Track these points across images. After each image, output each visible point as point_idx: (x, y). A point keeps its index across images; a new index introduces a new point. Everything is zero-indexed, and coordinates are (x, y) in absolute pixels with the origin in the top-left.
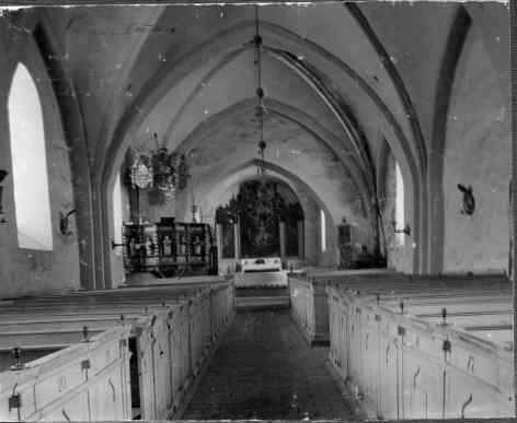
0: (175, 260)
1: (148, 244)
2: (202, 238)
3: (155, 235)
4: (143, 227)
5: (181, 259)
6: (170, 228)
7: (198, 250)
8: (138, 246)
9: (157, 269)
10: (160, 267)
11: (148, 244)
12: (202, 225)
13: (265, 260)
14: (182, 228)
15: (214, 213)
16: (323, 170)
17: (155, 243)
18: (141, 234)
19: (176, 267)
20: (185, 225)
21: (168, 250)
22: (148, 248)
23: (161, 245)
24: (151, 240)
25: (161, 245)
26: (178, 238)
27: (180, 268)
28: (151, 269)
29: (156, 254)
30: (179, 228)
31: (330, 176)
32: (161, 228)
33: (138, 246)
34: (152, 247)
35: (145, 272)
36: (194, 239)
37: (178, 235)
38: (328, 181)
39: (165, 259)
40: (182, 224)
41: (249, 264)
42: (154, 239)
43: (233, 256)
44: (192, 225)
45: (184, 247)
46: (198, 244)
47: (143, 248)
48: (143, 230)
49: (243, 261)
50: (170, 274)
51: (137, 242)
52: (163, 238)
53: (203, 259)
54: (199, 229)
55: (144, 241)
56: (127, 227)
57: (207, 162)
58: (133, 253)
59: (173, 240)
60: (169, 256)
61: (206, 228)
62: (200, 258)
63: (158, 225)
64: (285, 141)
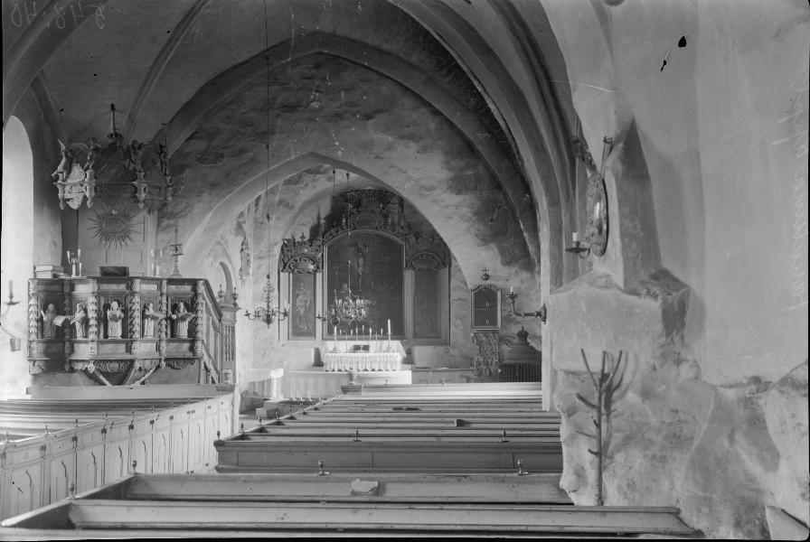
0: (129, 350)
1: (79, 315)
2: (192, 306)
3: (92, 299)
4: (72, 285)
5: (143, 349)
6: (122, 287)
7: (183, 329)
8: (59, 321)
9: (92, 368)
10: (96, 362)
11: (79, 315)
12: (194, 283)
13: (373, 344)
14: (154, 287)
15: (277, 250)
16: (445, 174)
17: (91, 315)
18: (71, 296)
19: (132, 361)
20: (159, 281)
21: (116, 330)
22: (78, 326)
23: (103, 321)
24: (86, 311)
25: (103, 321)
26: (137, 307)
27: (137, 365)
28: (79, 366)
29: (92, 337)
30: (138, 286)
31: (458, 185)
32: (105, 287)
33: (59, 321)
34: (85, 321)
35: (72, 370)
36: (175, 308)
37: (137, 299)
38: (454, 199)
39: (108, 348)
40: (145, 279)
41: (340, 352)
42: (91, 308)
43: (312, 334)
44: (170, 281)
45: (150, 326)
46: (183, 319)
47: (69, 327)
48: (72, 288)
49: (330, 345)
50: (120, 378)
51: (59, 312)
52: (107, 307)
53: (192, 349)
54: (188, 288)
55: (71, 313)
56: (41, 282)
58: (49, 333)
60: (115, 342)
61: (201, 289)
62: (186, 346)
63: (99, 281)
64: (368, 117)
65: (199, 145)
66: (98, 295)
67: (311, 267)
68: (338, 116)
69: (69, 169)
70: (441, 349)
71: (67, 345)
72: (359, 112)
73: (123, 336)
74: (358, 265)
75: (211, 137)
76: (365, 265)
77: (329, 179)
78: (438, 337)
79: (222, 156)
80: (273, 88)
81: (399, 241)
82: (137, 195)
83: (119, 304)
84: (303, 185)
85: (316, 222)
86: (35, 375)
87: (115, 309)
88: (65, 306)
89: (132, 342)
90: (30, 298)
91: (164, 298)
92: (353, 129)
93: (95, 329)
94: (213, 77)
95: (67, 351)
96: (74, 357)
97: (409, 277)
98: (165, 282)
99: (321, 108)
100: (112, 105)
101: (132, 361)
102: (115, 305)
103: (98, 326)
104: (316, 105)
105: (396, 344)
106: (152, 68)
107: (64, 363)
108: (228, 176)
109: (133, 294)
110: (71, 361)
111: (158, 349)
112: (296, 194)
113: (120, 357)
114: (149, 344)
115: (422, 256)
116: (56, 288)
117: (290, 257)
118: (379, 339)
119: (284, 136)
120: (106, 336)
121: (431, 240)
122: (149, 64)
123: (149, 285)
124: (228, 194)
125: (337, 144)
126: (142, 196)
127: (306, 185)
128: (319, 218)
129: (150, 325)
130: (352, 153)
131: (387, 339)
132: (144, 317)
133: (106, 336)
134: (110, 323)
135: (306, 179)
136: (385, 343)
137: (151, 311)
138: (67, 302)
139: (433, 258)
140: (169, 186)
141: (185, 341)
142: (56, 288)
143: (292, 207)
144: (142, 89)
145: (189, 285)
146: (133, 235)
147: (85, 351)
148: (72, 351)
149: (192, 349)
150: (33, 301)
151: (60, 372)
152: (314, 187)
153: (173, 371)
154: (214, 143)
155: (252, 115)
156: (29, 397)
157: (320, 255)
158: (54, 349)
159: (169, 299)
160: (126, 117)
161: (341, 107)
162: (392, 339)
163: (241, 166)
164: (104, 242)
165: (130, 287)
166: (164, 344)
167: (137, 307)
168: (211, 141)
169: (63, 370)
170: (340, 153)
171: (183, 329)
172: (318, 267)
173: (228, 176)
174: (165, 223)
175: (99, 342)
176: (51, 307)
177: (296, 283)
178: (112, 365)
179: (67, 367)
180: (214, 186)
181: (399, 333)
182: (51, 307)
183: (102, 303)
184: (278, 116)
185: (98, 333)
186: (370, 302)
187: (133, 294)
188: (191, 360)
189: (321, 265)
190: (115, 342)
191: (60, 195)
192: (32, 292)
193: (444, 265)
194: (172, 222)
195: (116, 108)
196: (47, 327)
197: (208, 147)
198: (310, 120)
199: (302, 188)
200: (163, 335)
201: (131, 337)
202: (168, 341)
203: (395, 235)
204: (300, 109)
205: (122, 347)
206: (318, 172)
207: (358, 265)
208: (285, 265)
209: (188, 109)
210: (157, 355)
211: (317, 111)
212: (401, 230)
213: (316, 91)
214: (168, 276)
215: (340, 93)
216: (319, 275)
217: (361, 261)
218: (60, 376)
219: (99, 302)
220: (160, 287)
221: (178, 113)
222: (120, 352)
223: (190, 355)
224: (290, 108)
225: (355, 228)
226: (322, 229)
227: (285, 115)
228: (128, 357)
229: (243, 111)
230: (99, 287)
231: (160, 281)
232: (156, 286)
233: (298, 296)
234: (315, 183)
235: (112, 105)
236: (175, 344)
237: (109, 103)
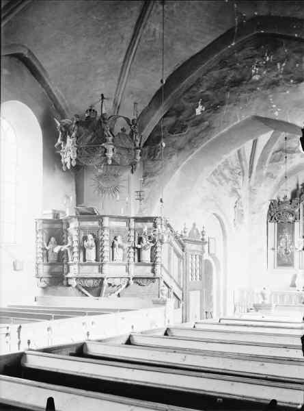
0: (101, 271)
6: (96, 224)
8: (57, 249)
14: (123, 224)
17: (76, 244)
19: (103, 279)
20: (127, 219)
21: (91, 255)
25: (83, 249)
27: (106, 282)
32: (84, 224)
36: (140, 240)
37: (106, 232)
42: (75, 239)
44: (137, 219)
52: (85, 238)
53: (153, 271)
57: (184, 128)
58: (52, 258)
59: (98, 243)
62: (150, 268)
65: (171, 121)
66: (79, 229)
67: (291, 219)
68: (274, 84)
69: (64, 140)
71: (65, 267)
72: (292, 78)
73: (96, 260)
75: (179, 113)
79: (186, 126)
80: (225, 70)
82: (106, 154)
83: (94, 236)
85: (295, 187)
86: (44, 288)
87: (91, 241)
88: (64, 238)
89: (102, 264)
90: (37, 233)
91: (132, 233)
92: (288, 92)
93: (76, 255)
94: (177, 68)
95: (65, 272)
96: (69, 275)
98: (132, 220)
99: (261, 79)
100: (102, 95)
101: (103, 279)
102: (90, 237)
103: (79, 252)
104: (256, 78)
106: (124, 62)
107: (63, 279)
108: (190, 141)
109: (103, 228)
110: (67, 278)
111: (127, 270)
112: (278, 168)
113: (94, 276)
114: (119, 267)
116: (57, 226)
117: (276, 212)
119: (231, 105)
120: (85, 260)
122: (122, 59)
123: (118, 223)
124: (190, 154)
125: (274, 106)
126: (110, 155)
128: (298, 185)
129: (119, 254)
130: (287, 112)
132: (113, 246)
133: (85, 260)
134: (87, 251)
137: (119, 242)
138: (65, 236)
140: (137, 149)
141: (148, 265)
142: (57, 226)
143: (275, 178)
144: (119, 80)
145: (151, 222)
146: (121, 189)
147: (73, 272)
148: (68, 271)
149: (153, 271)
150: (40, 235)
151: (61, 286)
152: (291, 162)
153: (140, 287)
154: (181, 117)
155: (208, 93)
156: (35, 304)
157: (297, 210)
158: (57, 269)
159: (136, 234)
160: (112, 104)
161: (277, 76)
163: (199, 133)
164: (101, 195)
165: (101, 224)
166: (132, 267)
167: (106, 238)
168: (178, 116)
169: (62, 285)
170: (276, 113)
171: (146, 256)
172: (296, 219)
173: (190, 141)
174: (148, 179)
175: (80, 264)
176: (53, 239)
177: (280, 230)
178: (89, 281)
179: (65, 282)
180: (180, 149)
182: (53, 239)
183: (82, 235)
184: (228, 90)
185: (79, 258)
187: (103, 228)
188: (153, 279)
189: (298, 217)
190: (91, 264)
191: (62, 161)
192: (38, 229)
194: (152, 179)
195: (105, 96)
196: (50, 253)
197: (177, 121)
198: (252, 90)
200: (132, 260)
201: (102, 261)
202: (136, 265)
204: (245, 82)
205: (96, 269)
208: (272, 217)
209: (159, 96)
210: (126, 275)
211: (258, 82)
213: (257, 67)
214: (133, 216)
215: (276, 64)
216: (296, 224)
218: (60, 288)
219: (79, 235)
220: (128, 225)
221: (153, 98)
222: (93, 272)
223: (151, 275)
224: (237, 83)
226: (299, 192)
227: (232, 89)
228: (100, 275)
229: (202, 91)
230: (79, 224)
231: (129, 219)
232: (125, 223)
233: (281, 238)
234: (293, 159)
235: (102, 95)
236: (141, 268)
237: (99, 93)
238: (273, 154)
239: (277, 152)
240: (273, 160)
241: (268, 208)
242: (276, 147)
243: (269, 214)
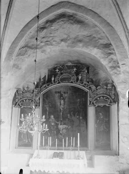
13: (65, 152)
70: (113, 158)
74: (61, 104)
76: (64, 104)
77: (43, 51)
78: (110, 149)
81: (86, 89)
84: (27, 56)
97: (91, 111)
105: (83, 153)
115: (100, 97)
118: (73, 150)
121: (105, 87)
127: (29, 56)
128: (40, 79)
131: (77, 150)
135: (29, 52)
136: (77, 152)
139: (108, 98)
157: (38, 98)
162: (80, 150)
181: (84, 145)
186: (67, 127)
189: (38, 105)
193: (115, 102)
199: (26, 57)
203: (83, 86)
206: (36, 48)
207: (61, 104)
212: (87, 83)
217: (62, 102)
225: (59, 83)
238: (20, 49)
239: (23, 47)
240: (19, 54)
241: (14, 95)
242: (22, 43)
243: (14, 99)
